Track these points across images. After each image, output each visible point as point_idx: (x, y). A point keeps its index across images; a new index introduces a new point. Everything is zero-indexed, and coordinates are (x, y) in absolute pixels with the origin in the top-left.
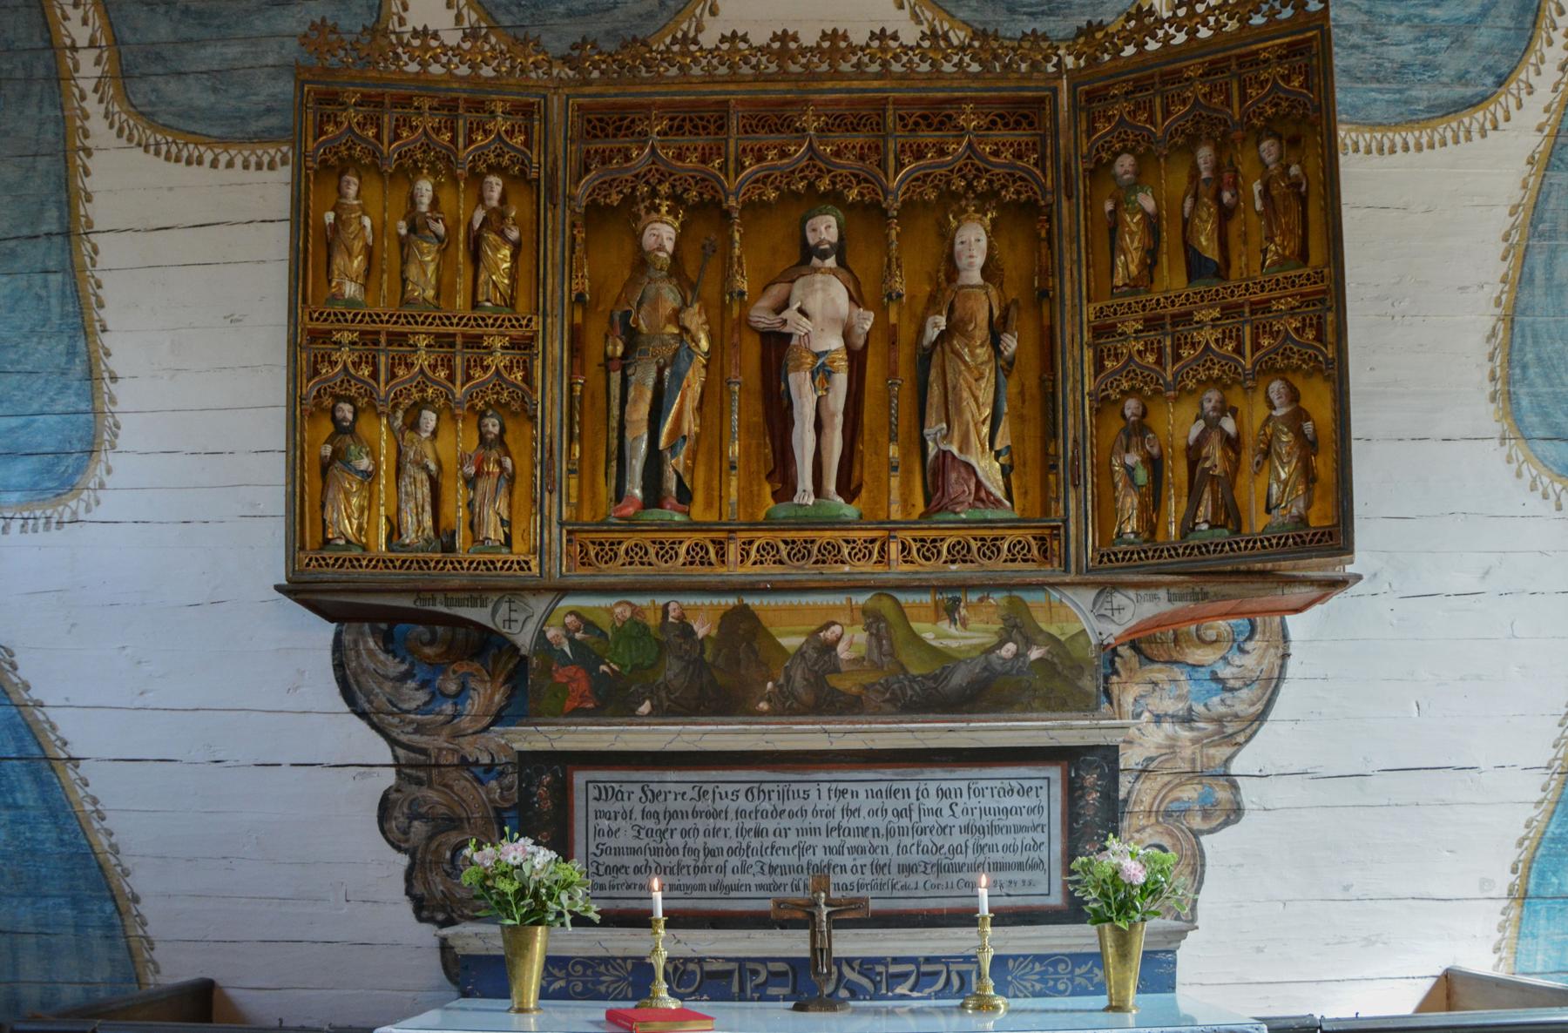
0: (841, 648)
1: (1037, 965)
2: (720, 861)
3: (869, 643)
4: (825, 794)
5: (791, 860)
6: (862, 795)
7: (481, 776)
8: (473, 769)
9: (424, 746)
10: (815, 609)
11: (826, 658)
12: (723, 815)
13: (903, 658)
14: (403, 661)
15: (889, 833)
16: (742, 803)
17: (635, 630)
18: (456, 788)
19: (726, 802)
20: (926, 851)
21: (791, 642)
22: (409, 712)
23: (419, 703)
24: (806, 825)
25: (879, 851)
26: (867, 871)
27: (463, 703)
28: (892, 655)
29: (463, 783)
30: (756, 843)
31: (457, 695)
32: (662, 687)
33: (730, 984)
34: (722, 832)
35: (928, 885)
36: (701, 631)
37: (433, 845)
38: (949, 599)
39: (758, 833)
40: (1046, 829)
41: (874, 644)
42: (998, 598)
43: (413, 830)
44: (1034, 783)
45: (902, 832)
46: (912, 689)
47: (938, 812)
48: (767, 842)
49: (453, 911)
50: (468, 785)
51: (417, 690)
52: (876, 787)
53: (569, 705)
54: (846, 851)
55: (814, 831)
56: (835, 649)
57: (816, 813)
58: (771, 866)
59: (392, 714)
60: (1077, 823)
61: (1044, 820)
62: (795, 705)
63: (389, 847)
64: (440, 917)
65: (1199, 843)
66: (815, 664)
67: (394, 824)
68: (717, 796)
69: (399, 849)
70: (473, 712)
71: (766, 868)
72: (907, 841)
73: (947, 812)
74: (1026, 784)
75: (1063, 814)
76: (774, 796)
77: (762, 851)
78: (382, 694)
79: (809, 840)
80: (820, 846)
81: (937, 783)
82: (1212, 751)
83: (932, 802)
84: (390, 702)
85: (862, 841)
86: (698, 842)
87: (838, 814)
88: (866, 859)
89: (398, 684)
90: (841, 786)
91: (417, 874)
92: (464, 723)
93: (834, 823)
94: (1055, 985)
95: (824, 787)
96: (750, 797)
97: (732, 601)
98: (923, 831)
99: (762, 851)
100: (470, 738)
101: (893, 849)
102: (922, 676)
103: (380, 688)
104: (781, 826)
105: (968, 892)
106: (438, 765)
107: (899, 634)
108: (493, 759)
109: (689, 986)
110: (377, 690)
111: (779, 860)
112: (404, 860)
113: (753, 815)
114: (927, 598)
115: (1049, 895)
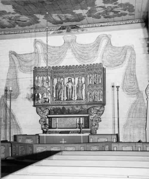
16: (63, 120)
17: (57, 108)
21: (67, 109)
36: (61, 108)
42: (80, 106)
53: (52, 114)
78: (40, 112)
86: (60, 123)
97: (63, 106)
114: (76, 106)
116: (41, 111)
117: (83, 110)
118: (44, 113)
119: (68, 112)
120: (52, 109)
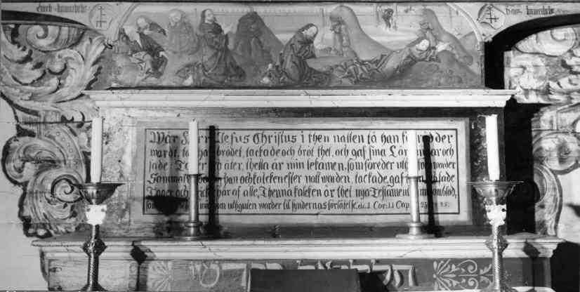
0: (316, 42)
1: (453, 266)
2: (235, 186)
3: (335, 39)
4: (306, 138)
5: (283, 186)
6: (332, 139)
7: (75, 129)
8: (70, 125)
9: (36, 109)
10: (301, 15)
11: (307, 48)
12: (238, 154)
13: (357, 50)
14: (24, 50)
15: (350, 167)
16: (251, 145)
18: (57, 138)
19: (240, 144)
20: (375, 180)
21: (284, 38)
22: (26, 84)
23: (34, 78)
24: (294, 161)
25: (343, 180)
26: (335, 194)
27: (65, 79)
28: (349, 47)
29: (62, 134)
30: (259, 173)
31: (61, 73)
32: (200, 66)
33: (239, 280)
34: (237, 166)
35: (377, 205)
36: (226, 30)
37: (40, 179)
38: (386, 10)
39: (262, 166)
40: (455, 166)
41: (337, 37)
43: (25, 169)
44: (447, 133)
45: (359, 166)
46: (363, 70)
47: (382, 153)
48: (268, 172)
49: (51, 228)
50: (66, 137)
51: (33, 69)
52: (341, 133)
54: (321, 180)
55: (300, 165)
56: (312, 42)
57: (301, 152)
58: (270, 191)
59: (13, 86)
60: (477, 162)
61: (454, 159)
62: (286, 80)
63: (7, 181)
64: (41, 232)
65: (557, 180)
66: (299, 52)
67: (12, 164)
68: (234, 139)
69: (15, 183)
70: (72, 84)
71: (267, 192)
72: (362, 173)
73: (388, 152)
74: (442, 133)
75: (467, 157)
76: (273, 140)
77: (264, 179)
79: (296, 171)
80: (303, 175)
81: (381, 132)
82: (564, 116)
83: (378, 145)
84: (15, 79)
85: (332, 173)
87: (315, 153)
88: (335, 186)
89: (20, 65)
90: (318, 133)
91: (27, 200)
92: (64, 92)
93: (312, 160)
94: (467, 282)
95: (306, 133)
96: (256, 141)
98: (373, 166)
99: (264, 179)
100: (67, 104)
101: (352, 179)
102: (370, 62)
103: (8, 68)
104: (277, 162)
105: (404, 211)
106: (45, 123)
107: (353, 33)
108: (84, 118)
109: (215, 280)
110: (5, 70)
111: (276, 186)
112: (19, 191)
113: (258, 154)
115: (458, 213)
116: (27, 59)
117: (441, 47)
118: (54, 81)
119: (301, 63)
120: (130, 30)
